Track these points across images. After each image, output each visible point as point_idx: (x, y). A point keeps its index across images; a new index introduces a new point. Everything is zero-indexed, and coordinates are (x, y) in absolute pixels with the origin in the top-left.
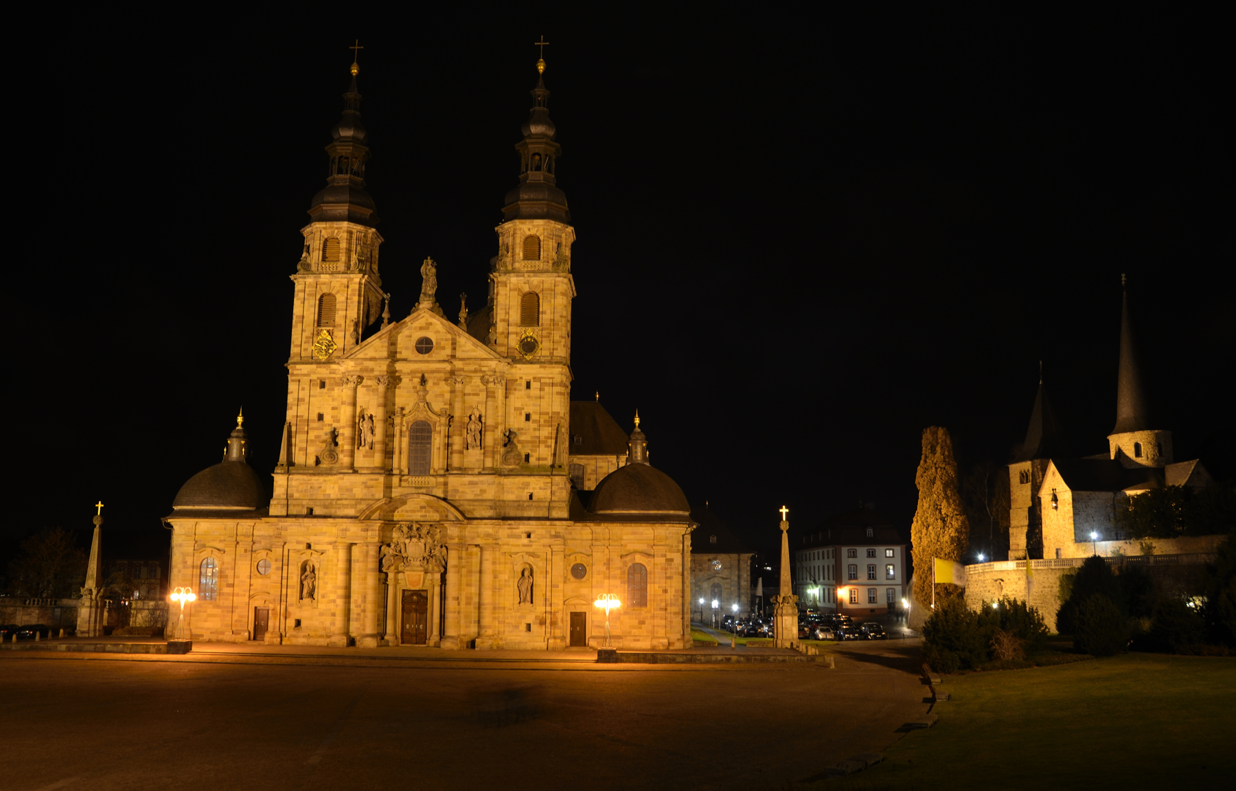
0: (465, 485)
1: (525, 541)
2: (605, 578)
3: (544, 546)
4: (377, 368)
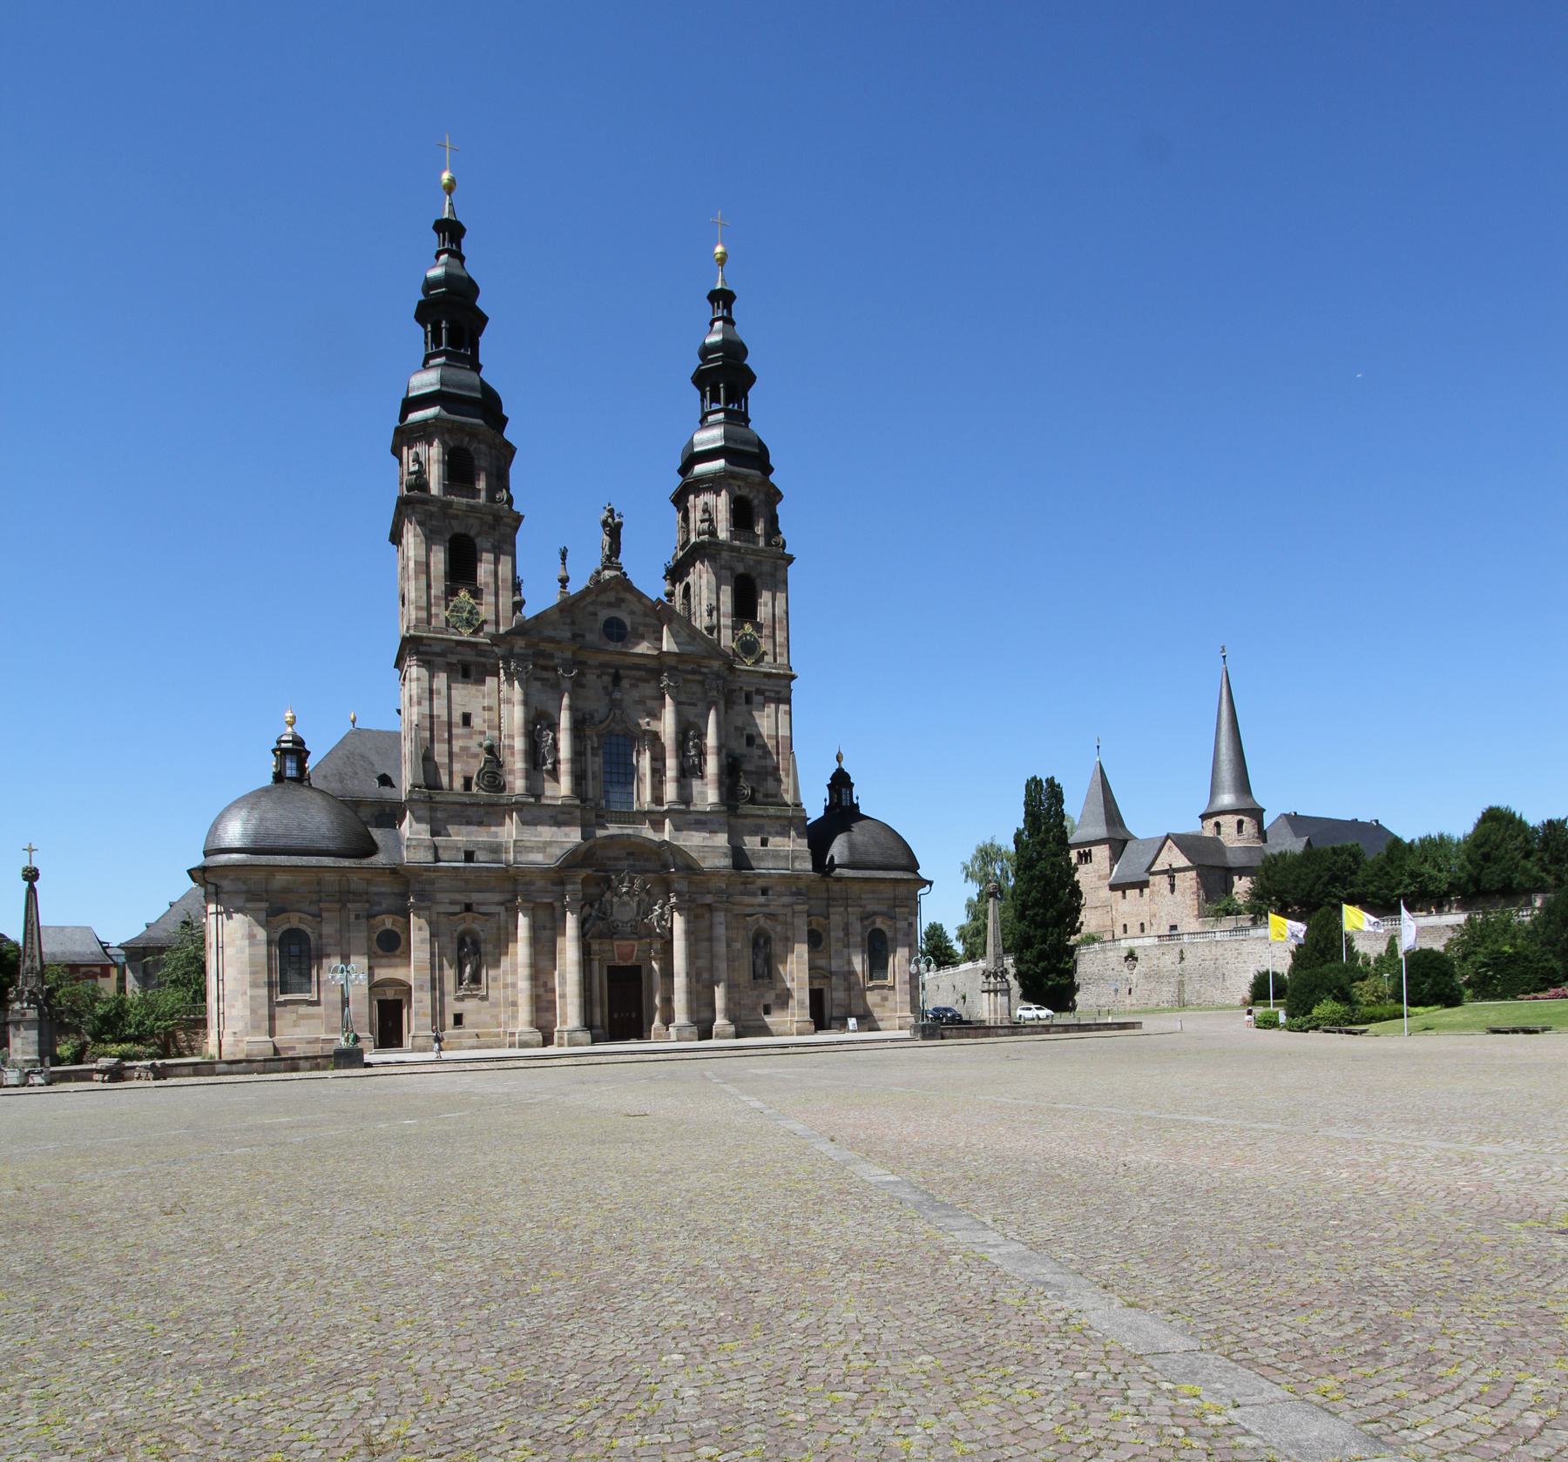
1: (761, 899)
2: (844, 947)
3: (783, 906)
4: (558, 654)
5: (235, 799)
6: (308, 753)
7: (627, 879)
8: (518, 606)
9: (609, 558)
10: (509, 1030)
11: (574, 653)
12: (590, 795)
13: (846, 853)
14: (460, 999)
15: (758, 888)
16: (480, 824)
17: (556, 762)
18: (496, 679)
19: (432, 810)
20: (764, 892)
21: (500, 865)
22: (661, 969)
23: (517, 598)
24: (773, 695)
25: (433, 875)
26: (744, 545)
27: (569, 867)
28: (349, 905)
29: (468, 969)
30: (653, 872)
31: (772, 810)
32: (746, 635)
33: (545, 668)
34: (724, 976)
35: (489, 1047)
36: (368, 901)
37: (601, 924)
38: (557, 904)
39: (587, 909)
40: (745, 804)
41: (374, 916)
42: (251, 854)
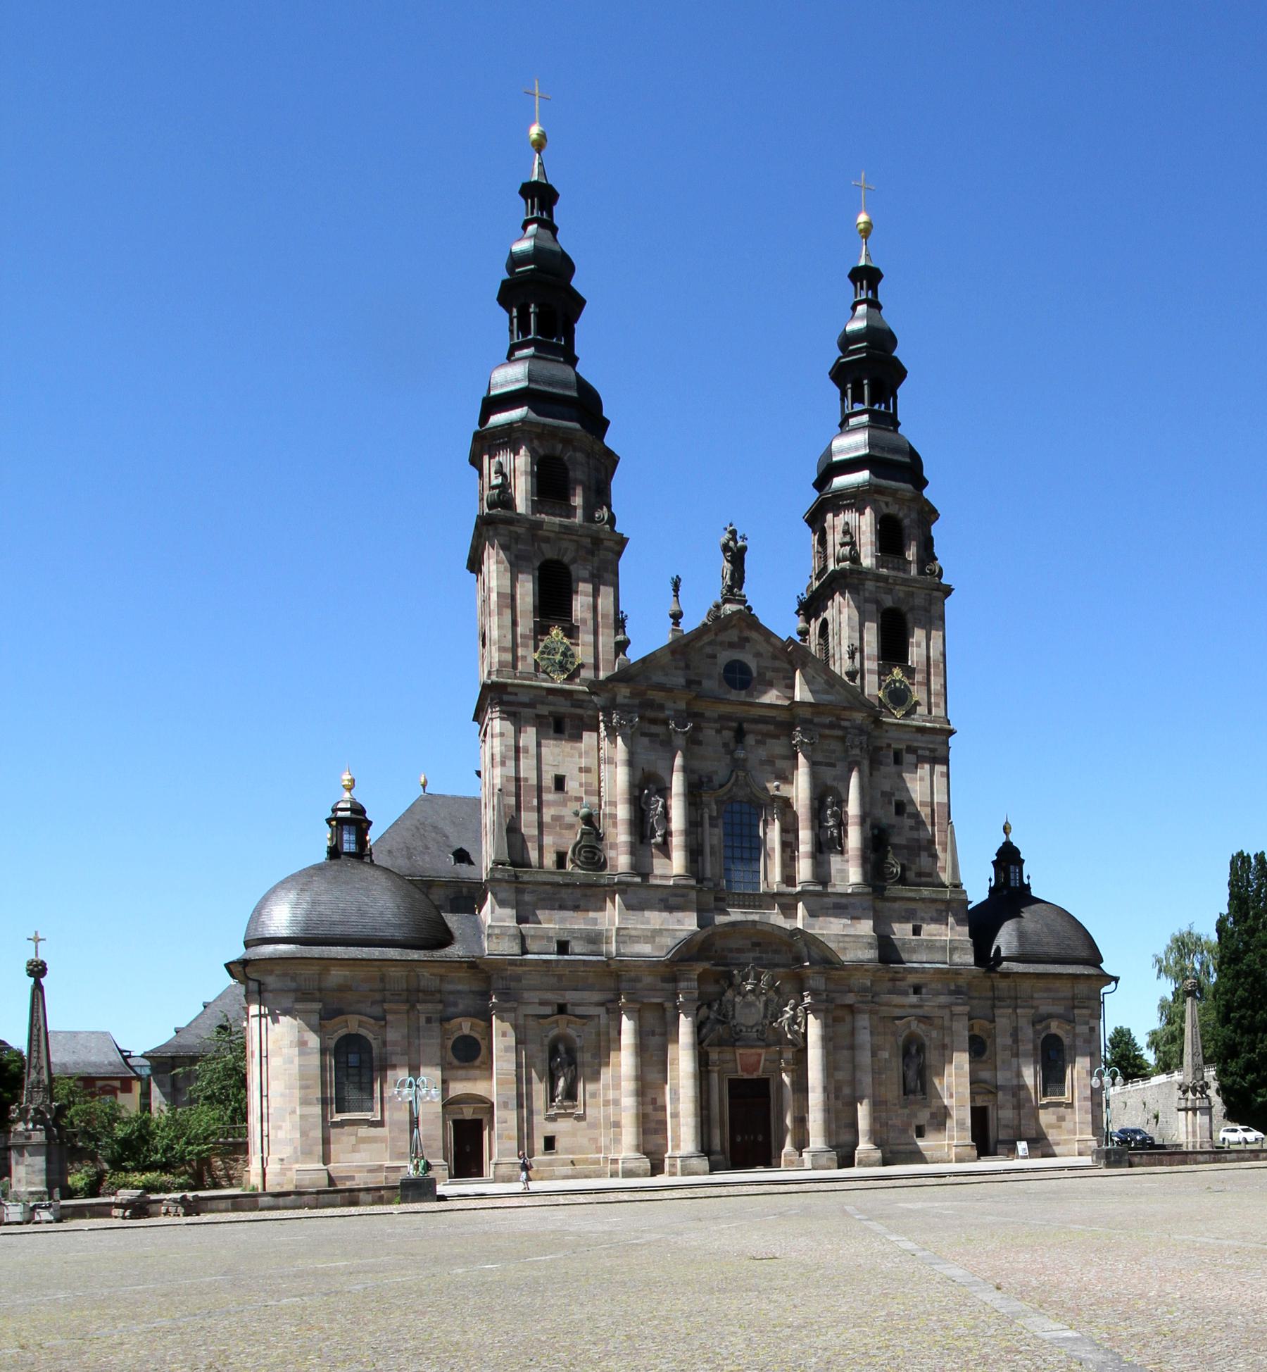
0: (828, 909)
1: (913, 999)
3: (939, 1007)
4: (669, 704)
5: (281, 878)
6: (370, 823)
7: (752, 974)
8: (622, 647)
9: (730, 589)
10: (611, 1156)
11: (688, 704)
12: (708, 874)
13: (1015, 943)
14: (552, 1119)
15: (909, 986)
16: (576, 908)
17: (667, 834)
18: (595, 734)
19: (519, 891)
20: (917, 990)
21: (599, 958)
22: (793, 1083)
23: (620, 638)
24: (927, 753)
25: (520, 970)
26: (892, 573)
27: (682, 960)
28: (419, 1007)
29: (561, 1083)
30: (784, 966)
31: (926, 892)
32: (895, 681)
33: (654, 721)
34: (869, 1091)
35: (586, 1177)
36: (441, 1002)
37: (720, 1029)
38: (668, 1005)
39: (704, 1010)
40: (893, 884)
41: (448, 1019)
42: (301, 944)
